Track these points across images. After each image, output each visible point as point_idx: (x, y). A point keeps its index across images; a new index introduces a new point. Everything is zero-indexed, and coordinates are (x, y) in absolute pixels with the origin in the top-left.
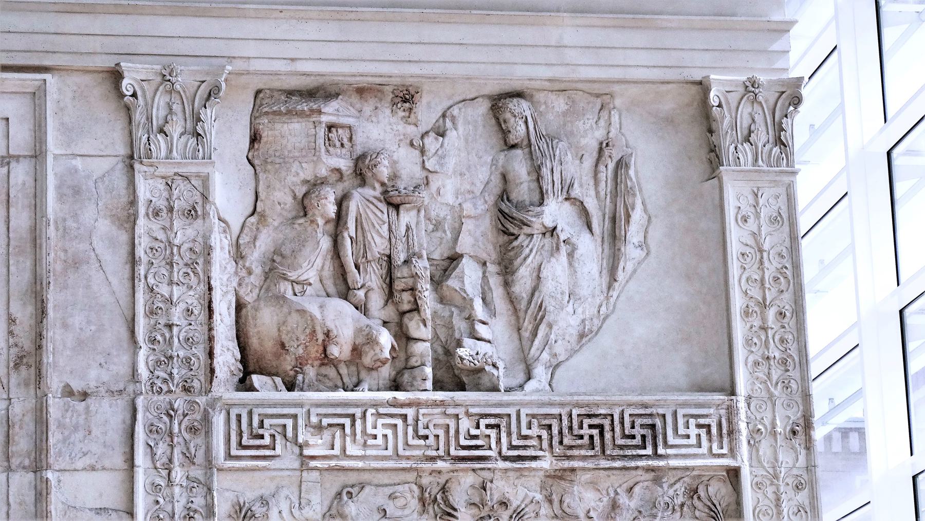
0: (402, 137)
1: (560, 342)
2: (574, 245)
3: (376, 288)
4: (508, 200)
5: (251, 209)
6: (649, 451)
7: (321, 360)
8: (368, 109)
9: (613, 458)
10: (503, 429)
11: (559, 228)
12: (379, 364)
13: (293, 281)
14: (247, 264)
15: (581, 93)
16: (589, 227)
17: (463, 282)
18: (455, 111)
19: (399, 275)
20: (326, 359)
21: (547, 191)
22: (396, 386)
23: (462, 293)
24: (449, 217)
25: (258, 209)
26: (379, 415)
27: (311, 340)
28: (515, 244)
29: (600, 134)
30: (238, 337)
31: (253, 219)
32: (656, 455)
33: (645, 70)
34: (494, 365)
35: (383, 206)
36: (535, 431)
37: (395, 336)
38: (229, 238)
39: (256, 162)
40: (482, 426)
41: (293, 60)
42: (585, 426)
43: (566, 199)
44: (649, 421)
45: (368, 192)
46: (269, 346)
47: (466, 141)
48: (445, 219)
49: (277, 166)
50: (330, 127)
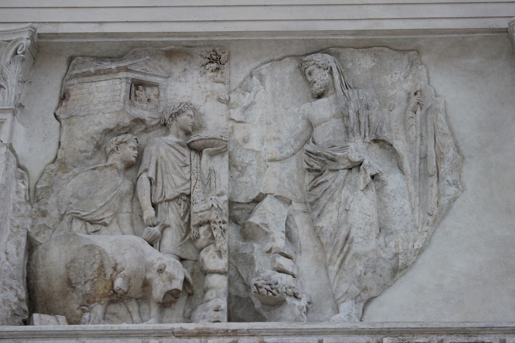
0: (209, 93)
1: (369, 274)
2: (383, 181)
3: (173, 225)
4: (314, 142)
5: (53, 157)
7: (110, 297)
8: (177, 71)
11: (366, 162)
12: (170, 298)
14: (43, 208)
15: (386, 49)
16: (401, 168)
17: (265, 218)
18: (264, 70)
19: (196, 210)
20: (116, 298)
21: (353, 130)
22: (188, 319)
23: (264, 228)
24: (254, 163)
25: (59, 157)
27: (99, 274)
28: (321, 179)
29: (408, 86)
30: (28, 280)
31: (53, 167)
33: (449, 21)
34: (295, 296)
35: (186, 152)
37: (192, 274)
38: (27, 183)
39: (62, 116)
41: (100, 23)
43: (376, 141)
45: (172, 138)
46: (57, 284)
47: (274, 95)
48: (249, 164)
49: (82, 118)
50: (137, 85)
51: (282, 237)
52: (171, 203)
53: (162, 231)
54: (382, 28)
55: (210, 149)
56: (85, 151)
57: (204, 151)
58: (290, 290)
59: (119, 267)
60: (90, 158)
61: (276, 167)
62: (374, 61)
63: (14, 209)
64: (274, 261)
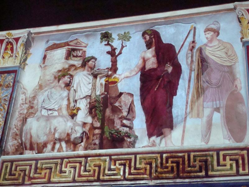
6: (203, 173)
9: (184, 178)
10: (127, 165)
13: (47, 109)
14: (32, 105)
17: (120, 103)
23: (119, 107)
26: (70, 162)
32: (207, 176)
36: (143, 166)
40: (117, 165)
42: (170, 162)
44: (205, 158)
51: (126, 111)
52: (83, 99)
53: (77, 112)
54: (176, 15)
55: (100, 75)
56: (50, 80)
57: (98, 76)
58: (126, 134)
59: (57, 129)
60: (51, 83)
61: (128, 80)
62: (175, 30)
63: (20, 106)
64: (121, 122)
